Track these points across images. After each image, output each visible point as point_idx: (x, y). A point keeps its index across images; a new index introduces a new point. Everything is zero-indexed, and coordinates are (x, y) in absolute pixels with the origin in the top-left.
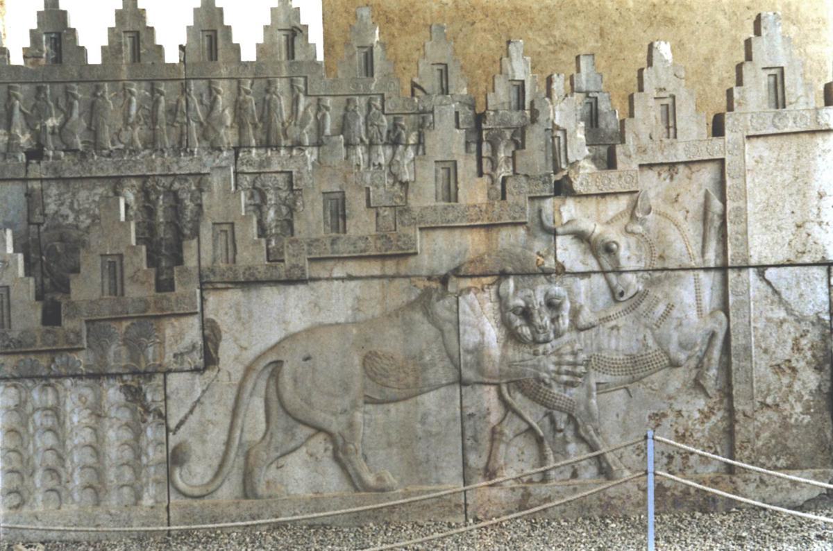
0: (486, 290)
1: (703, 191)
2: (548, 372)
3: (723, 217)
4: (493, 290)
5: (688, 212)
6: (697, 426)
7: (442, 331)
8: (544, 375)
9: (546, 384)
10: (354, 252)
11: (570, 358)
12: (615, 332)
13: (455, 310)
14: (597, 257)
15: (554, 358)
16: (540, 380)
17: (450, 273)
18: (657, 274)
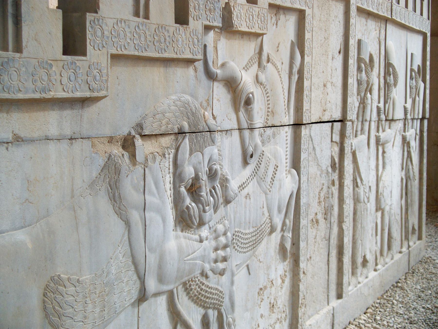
0: (167, 156)
1: (290, 43)
2: (209, 262)
3: (301, 72)
4: (172, 156)
5: (282, 63)
6: (280, 293)
7: (128, 224)
8: (207, 266)
9: (207, 277)
10: (35, 91)
11: (223, 240)
12: (248, 200)
13: (142, 190)
14: (237, 110)
15: (214, 244)
16: (204, 274)
17: (133, 133)
18: (269, 131)
